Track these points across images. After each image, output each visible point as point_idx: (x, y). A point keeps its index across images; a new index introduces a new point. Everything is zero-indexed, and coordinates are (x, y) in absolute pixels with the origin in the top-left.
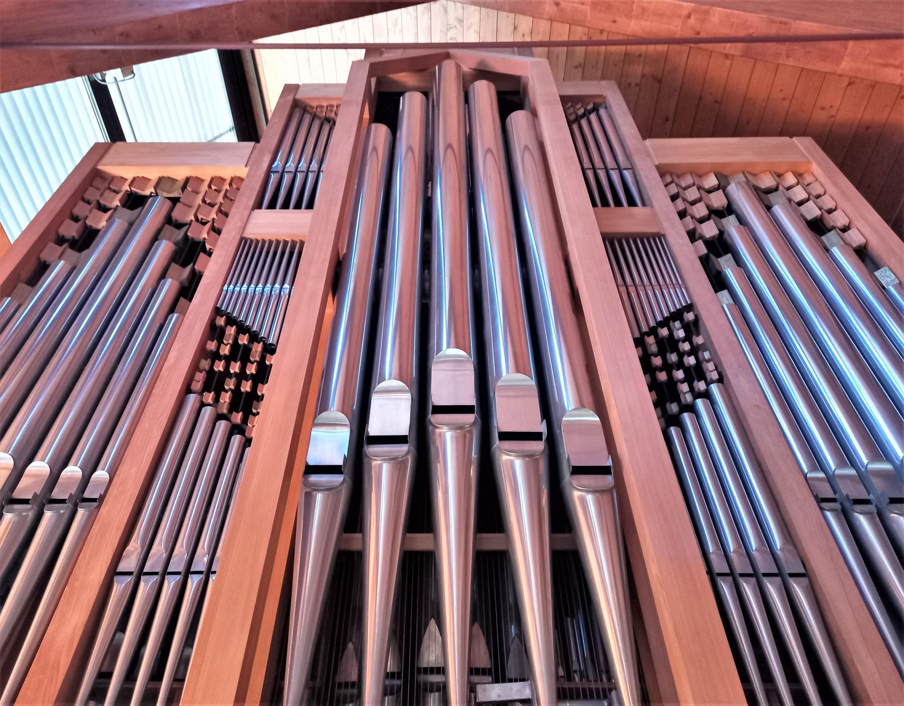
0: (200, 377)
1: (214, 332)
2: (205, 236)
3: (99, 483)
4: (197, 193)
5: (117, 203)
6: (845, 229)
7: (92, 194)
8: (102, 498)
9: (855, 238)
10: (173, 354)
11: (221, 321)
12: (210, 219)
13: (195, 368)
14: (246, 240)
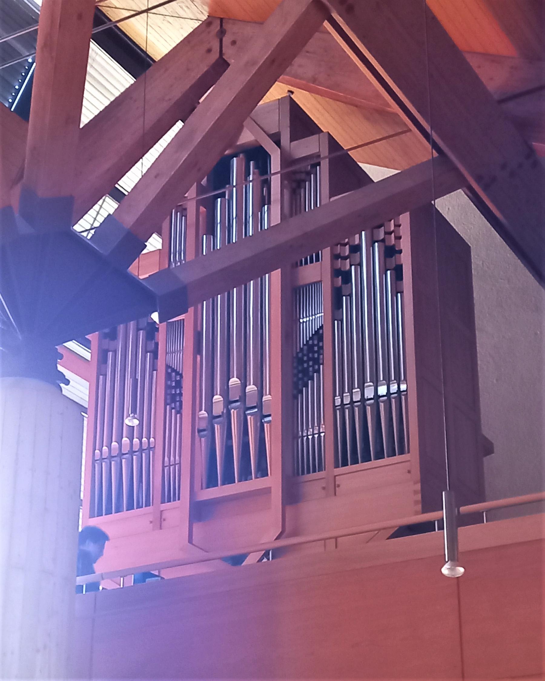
0: (168, 397)
1: (168, 376)
10: (158, 391)
13: (166, 394)
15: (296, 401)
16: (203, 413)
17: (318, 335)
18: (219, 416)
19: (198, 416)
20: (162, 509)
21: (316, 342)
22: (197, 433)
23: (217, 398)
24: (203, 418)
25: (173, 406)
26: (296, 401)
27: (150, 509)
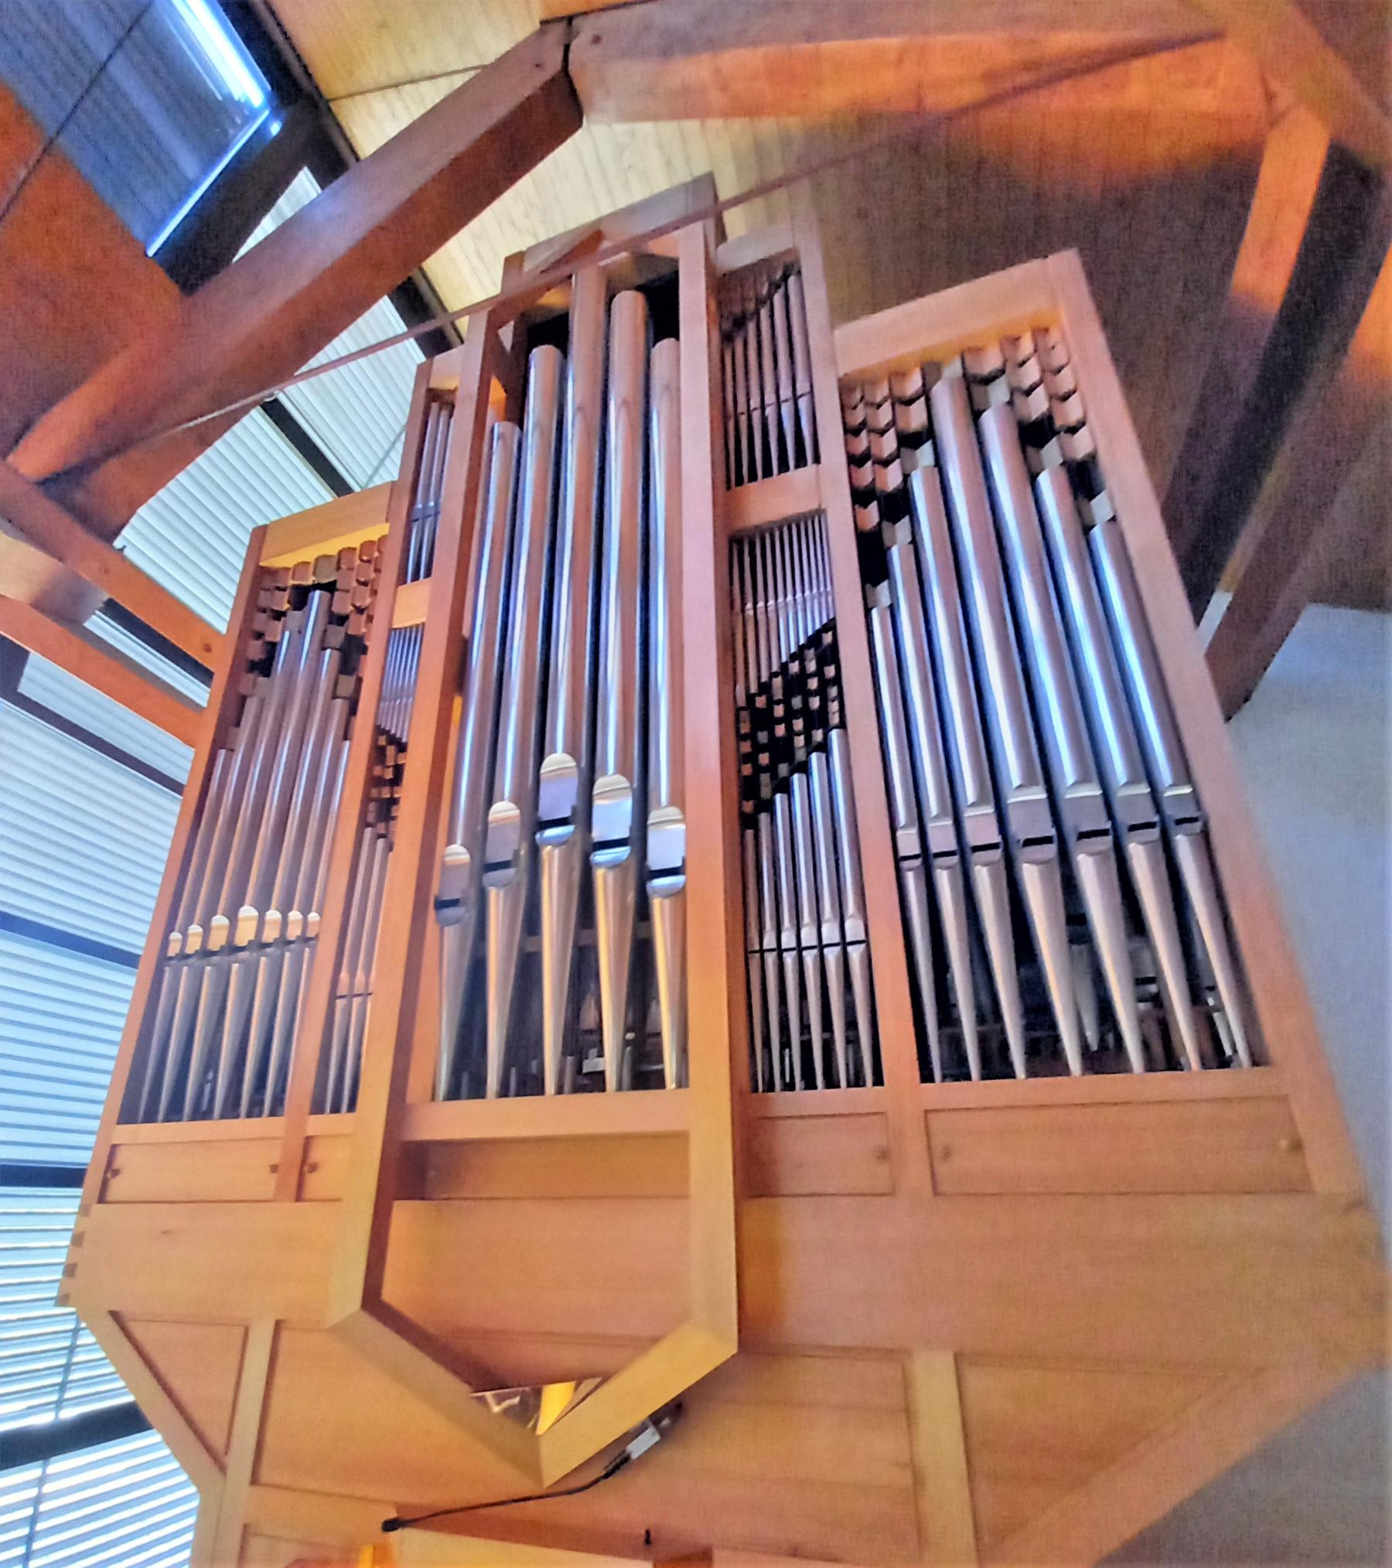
0: (372, 806)
1: (378, 754)
5: (287, 606)
7: (264, 599)
8: (316, 937)
11: (382, 741)
13: (367, 799)
15: (750, 833)
16: (458, 853)
17: (823, 647)
18: (505, 865)
19: (444, 856)
20: (310, 1133)
21: (812, 666)
22: (431, 913)
23: (504, 809)
24: (457, 867)
25: (383, 831)
26: (750, 833)
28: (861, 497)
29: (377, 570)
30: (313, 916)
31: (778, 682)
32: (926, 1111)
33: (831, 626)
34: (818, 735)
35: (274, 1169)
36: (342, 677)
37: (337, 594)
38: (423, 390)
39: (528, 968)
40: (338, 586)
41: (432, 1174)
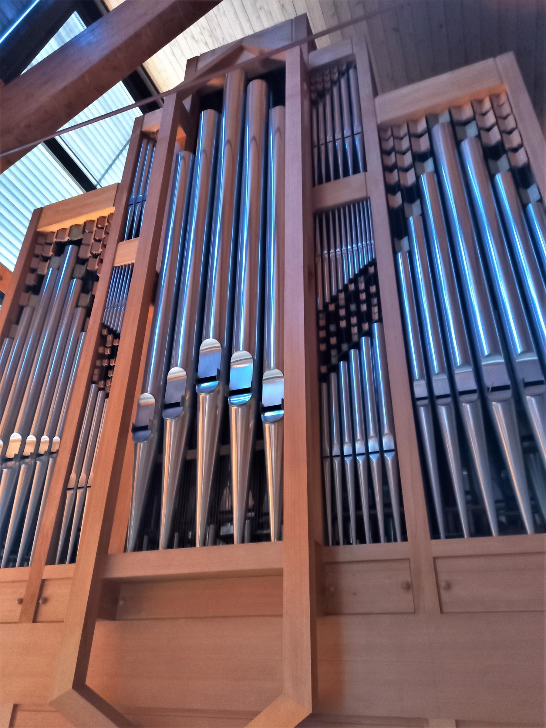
0: (96, 371)
1: (102, 340)
2: (97, 267)
3: (56, 443)
4: (92, 233)
5: (51, 253)
6: (515, 150)
7: (38, 250)
9: (521, 158)
10: (82, 360)
11: (105, 332)
12: (100, 252)
13: (93, 366)
14: (116, 267)
15: (324, 386)
16: (148, 398)
18: (177, 405)
19: (139, 400)
20: (44, 577)
21: (362, 286)
22: (130, 434)
23: (177, 372)
24: (147, 406)
27: (17, 573)
28: (391, 189)
29: (107, 233)
30: (56, 439)
31: (342, 296)
32: (435, 559)
33: (373, 263)
34: (366, 326)
35: (21, 601)
36: (83, 295)
37: (82, 246)
38: (138, 132)
39: (188, 468)
40: (83, 242)
41: (121, 603)
